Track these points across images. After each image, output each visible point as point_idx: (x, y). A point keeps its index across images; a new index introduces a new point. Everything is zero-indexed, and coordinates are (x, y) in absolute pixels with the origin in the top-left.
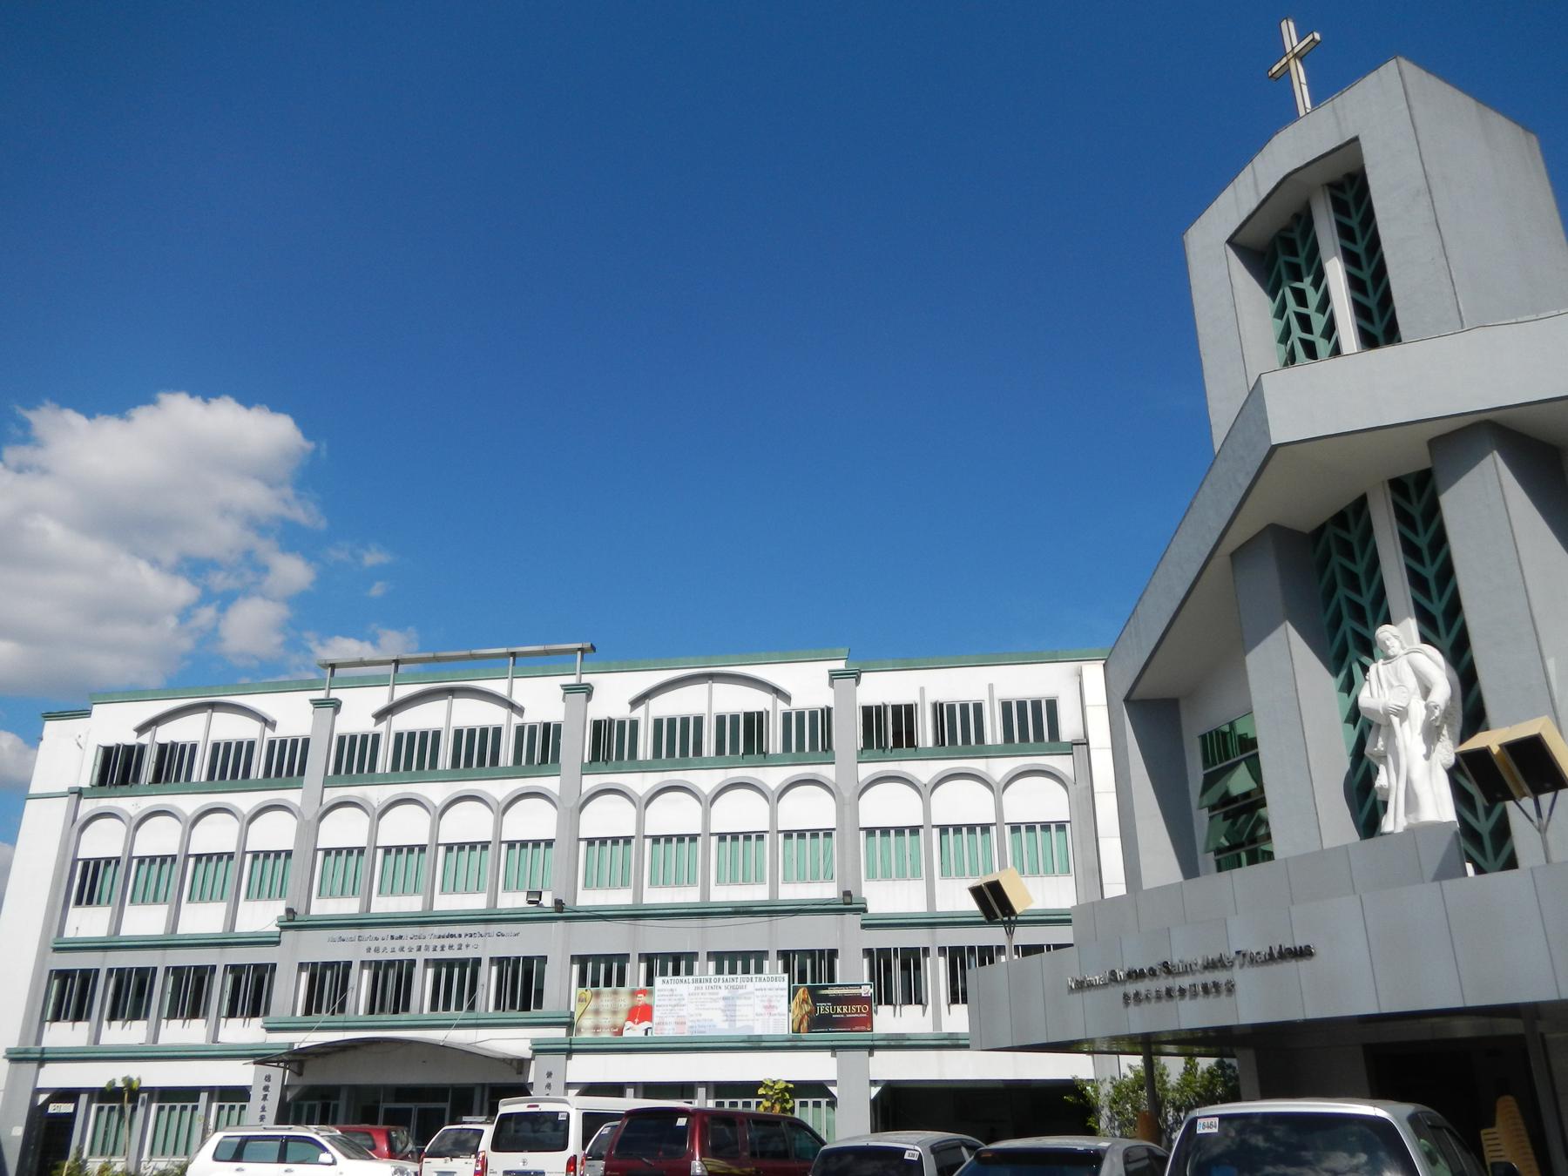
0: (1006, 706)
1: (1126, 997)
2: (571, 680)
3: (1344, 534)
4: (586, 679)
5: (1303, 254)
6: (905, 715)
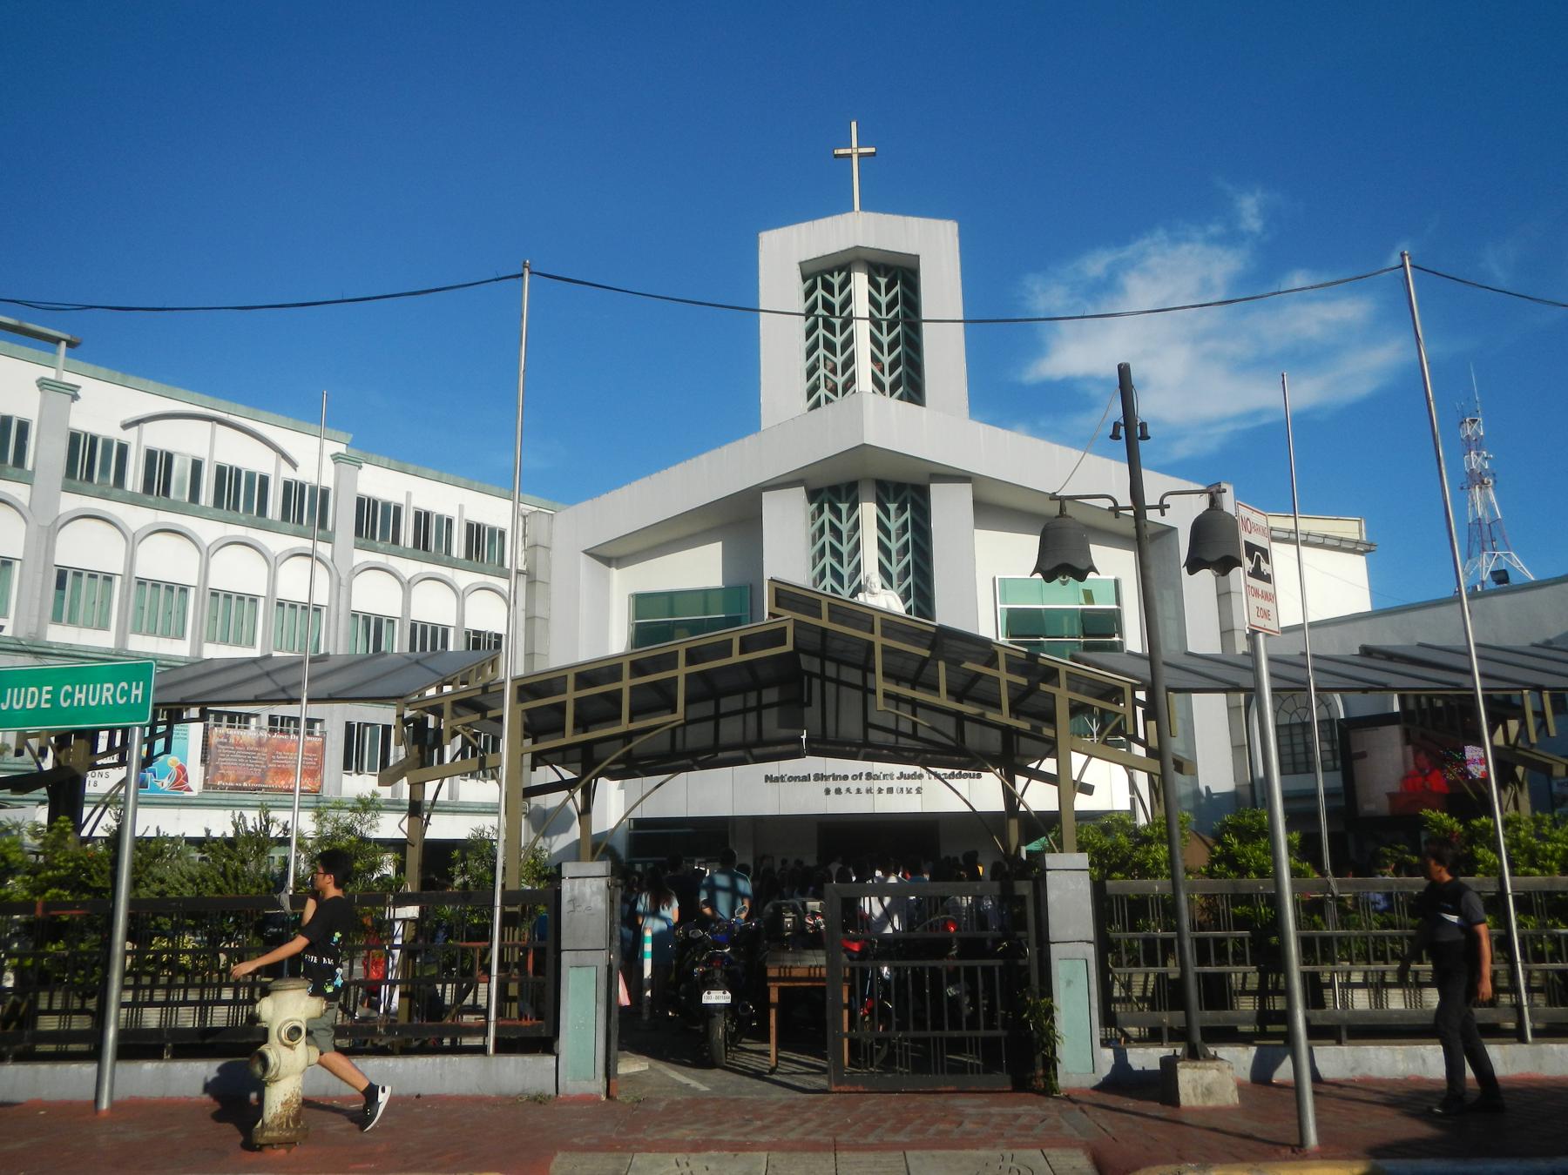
1: (828, 792)
2: (50, 374)
4: (69, 378)
6: (394, 513)
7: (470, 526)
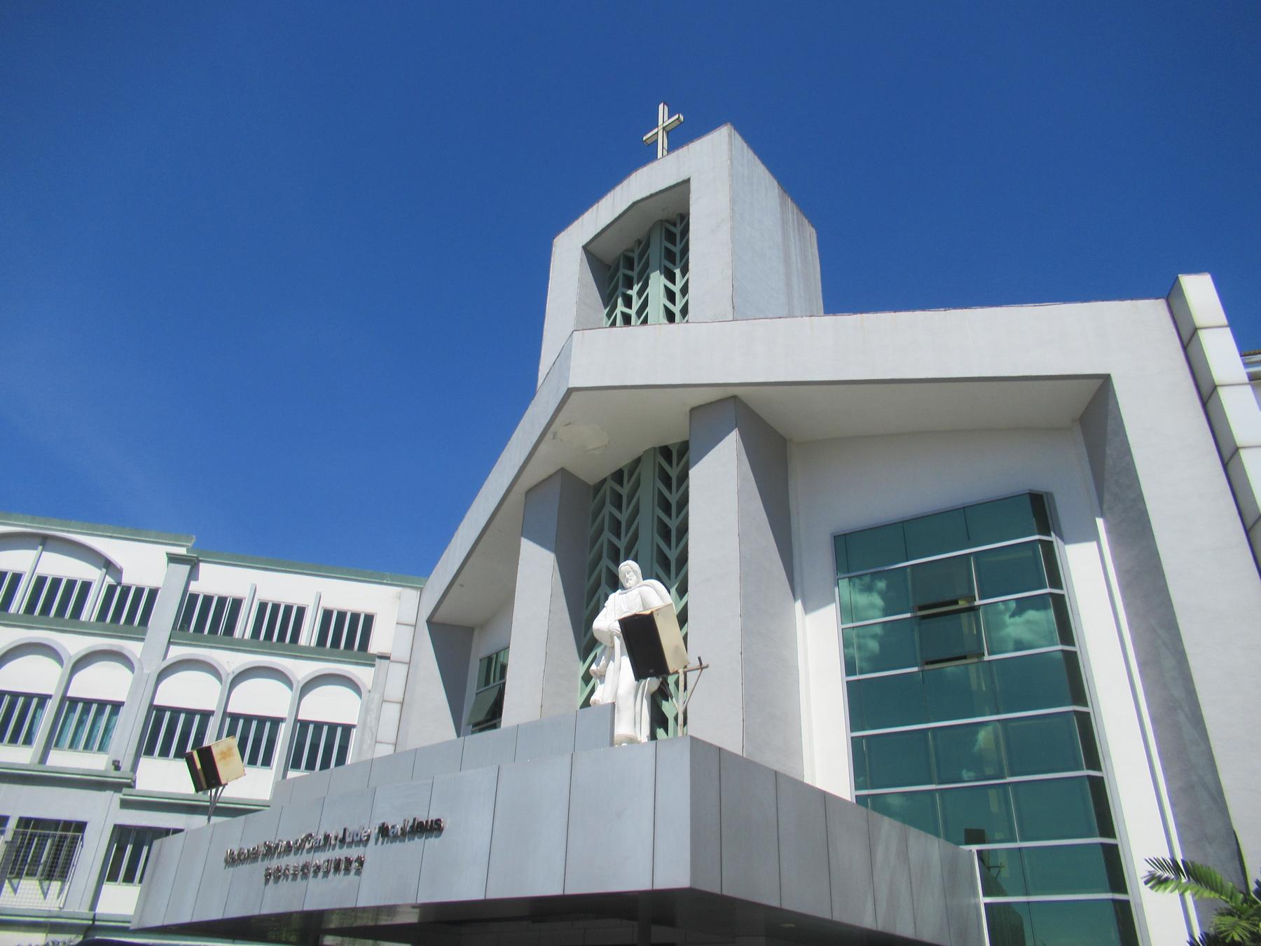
0: (327, 614)
3: (618, 488)
5: (637, 269)
7: (327, 614)
